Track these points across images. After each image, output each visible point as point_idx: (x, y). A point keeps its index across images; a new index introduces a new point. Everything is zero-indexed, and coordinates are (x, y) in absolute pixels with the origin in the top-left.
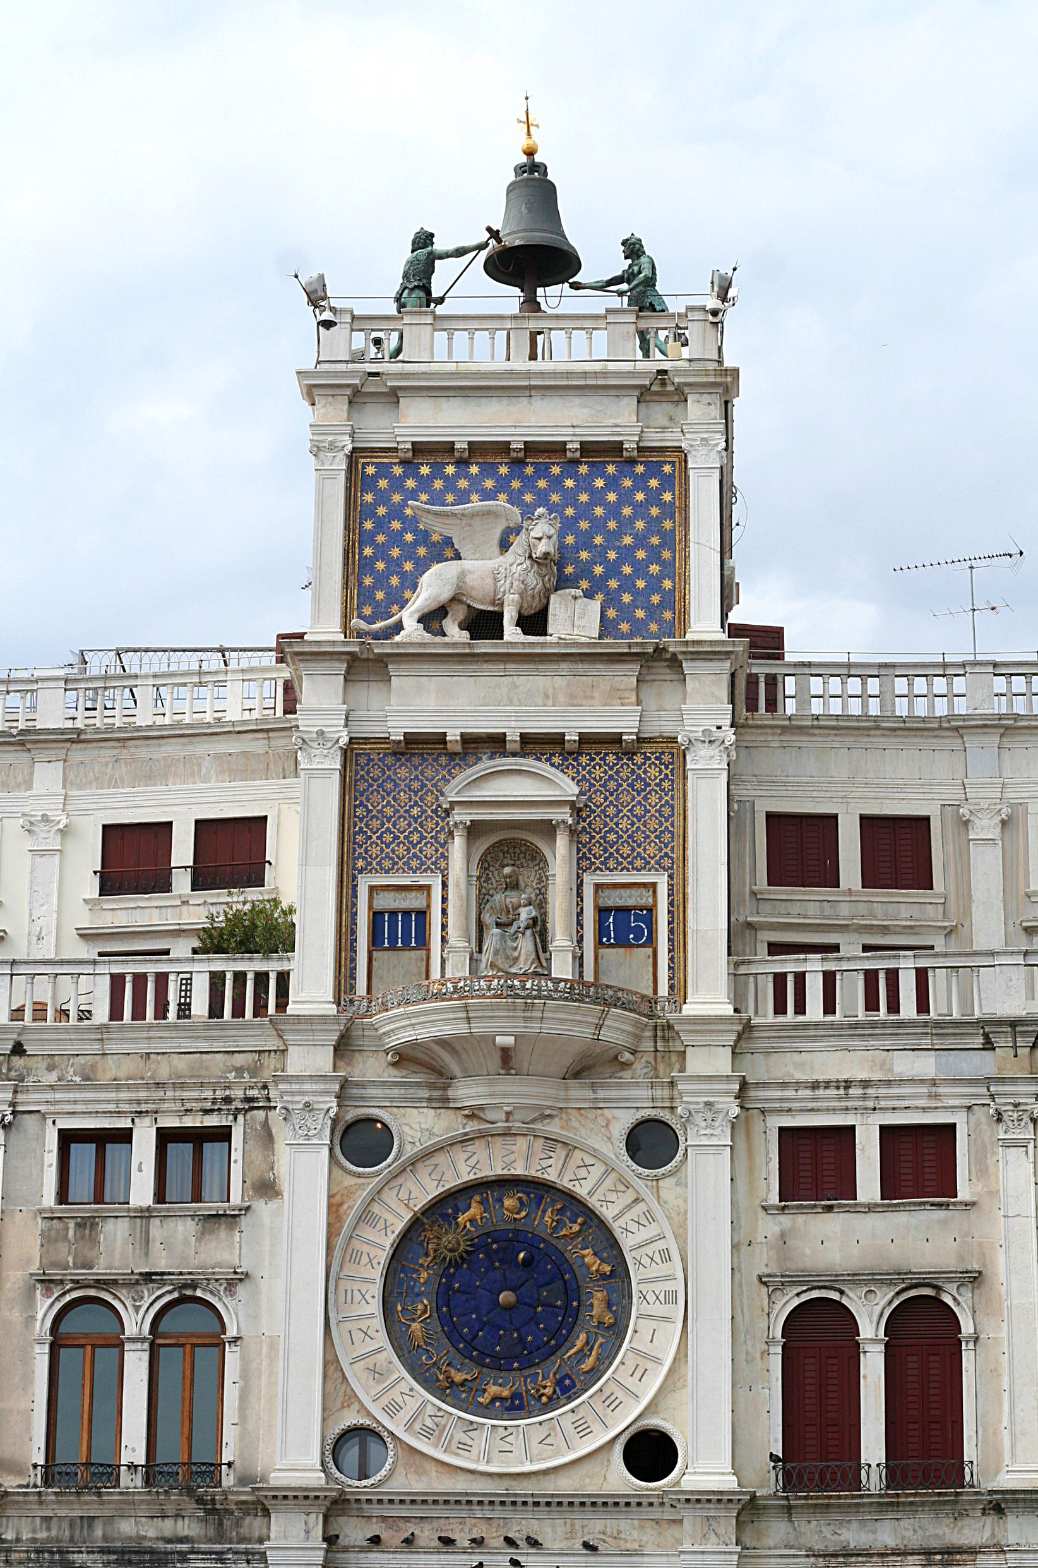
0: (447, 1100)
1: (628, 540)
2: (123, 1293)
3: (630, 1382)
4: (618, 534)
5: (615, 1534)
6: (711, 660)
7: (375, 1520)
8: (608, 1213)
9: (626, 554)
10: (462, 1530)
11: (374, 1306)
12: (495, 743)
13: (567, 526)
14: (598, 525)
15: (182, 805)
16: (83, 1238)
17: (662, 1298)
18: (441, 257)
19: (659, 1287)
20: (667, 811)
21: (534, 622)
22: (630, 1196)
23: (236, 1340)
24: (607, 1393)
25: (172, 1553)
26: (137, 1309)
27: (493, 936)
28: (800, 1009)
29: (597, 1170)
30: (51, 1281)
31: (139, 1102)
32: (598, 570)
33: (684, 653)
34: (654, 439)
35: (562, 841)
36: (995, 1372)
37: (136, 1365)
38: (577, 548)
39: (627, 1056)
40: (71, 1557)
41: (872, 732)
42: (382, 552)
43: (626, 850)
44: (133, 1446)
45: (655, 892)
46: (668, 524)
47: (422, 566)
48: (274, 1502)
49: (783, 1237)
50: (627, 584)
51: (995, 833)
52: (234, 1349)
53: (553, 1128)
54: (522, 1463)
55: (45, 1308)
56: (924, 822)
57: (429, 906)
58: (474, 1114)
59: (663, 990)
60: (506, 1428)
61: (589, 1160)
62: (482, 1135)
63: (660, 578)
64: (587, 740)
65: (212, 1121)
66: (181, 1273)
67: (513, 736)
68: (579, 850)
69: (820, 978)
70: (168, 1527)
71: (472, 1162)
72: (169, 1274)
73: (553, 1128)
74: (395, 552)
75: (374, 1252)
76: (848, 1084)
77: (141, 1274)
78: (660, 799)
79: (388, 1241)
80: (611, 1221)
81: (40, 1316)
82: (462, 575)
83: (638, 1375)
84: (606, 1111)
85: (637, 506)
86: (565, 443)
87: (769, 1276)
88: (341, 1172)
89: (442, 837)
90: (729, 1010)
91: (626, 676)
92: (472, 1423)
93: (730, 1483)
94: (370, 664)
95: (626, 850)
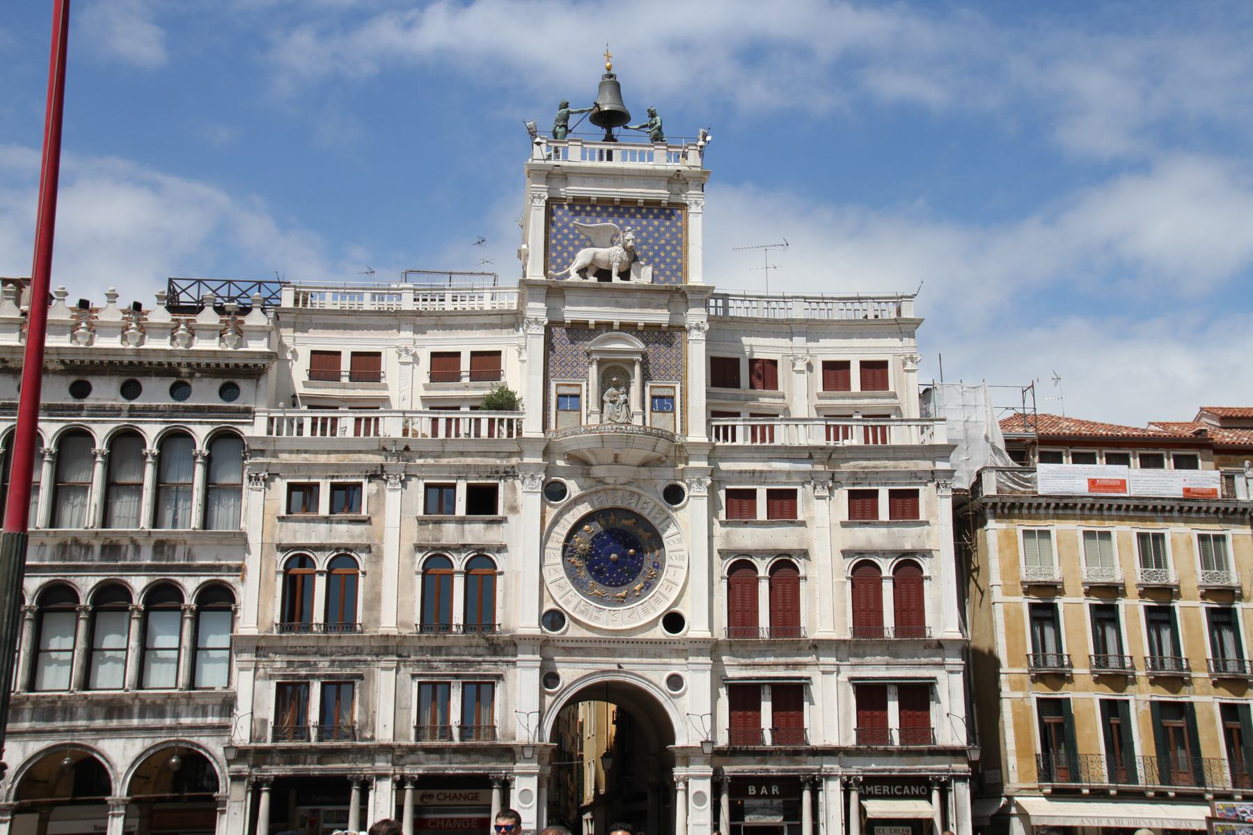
1: (663, 242)
3: (665, 593)
4: (658, 239)
8: (655, 523)
9: (662, 248)
11: (559, 560)
12: (609, 326)
13: (637, 234)
14: (650, 235)
15: (465, 343)
21: (625, 275)
22: (664, 516)
23: (501, 573)
27: (608, 406)
28: (734, 440)
29: (651, 506)
32: (651, 254)
34: (675, 200)
35: (637, 369)
37: (459, 584)
38: (642, 244)
42: (559, 242)
44: (458, 616)
47: (577, 249)
49: (727, 534)
50: (663, 260)
51: (804, 368)
55: (420, 558)
56: (774, 363)
58: (600, 481)
59: (678, 431)
63: (676, 258)
64: (647, 325)
67: (616, 324)
74: (565, 243)
76: (754, 472)
79: (565, 533)
82: (595, 254)
85: (667, 227)
90: (706, 440)
93: (708, 635)
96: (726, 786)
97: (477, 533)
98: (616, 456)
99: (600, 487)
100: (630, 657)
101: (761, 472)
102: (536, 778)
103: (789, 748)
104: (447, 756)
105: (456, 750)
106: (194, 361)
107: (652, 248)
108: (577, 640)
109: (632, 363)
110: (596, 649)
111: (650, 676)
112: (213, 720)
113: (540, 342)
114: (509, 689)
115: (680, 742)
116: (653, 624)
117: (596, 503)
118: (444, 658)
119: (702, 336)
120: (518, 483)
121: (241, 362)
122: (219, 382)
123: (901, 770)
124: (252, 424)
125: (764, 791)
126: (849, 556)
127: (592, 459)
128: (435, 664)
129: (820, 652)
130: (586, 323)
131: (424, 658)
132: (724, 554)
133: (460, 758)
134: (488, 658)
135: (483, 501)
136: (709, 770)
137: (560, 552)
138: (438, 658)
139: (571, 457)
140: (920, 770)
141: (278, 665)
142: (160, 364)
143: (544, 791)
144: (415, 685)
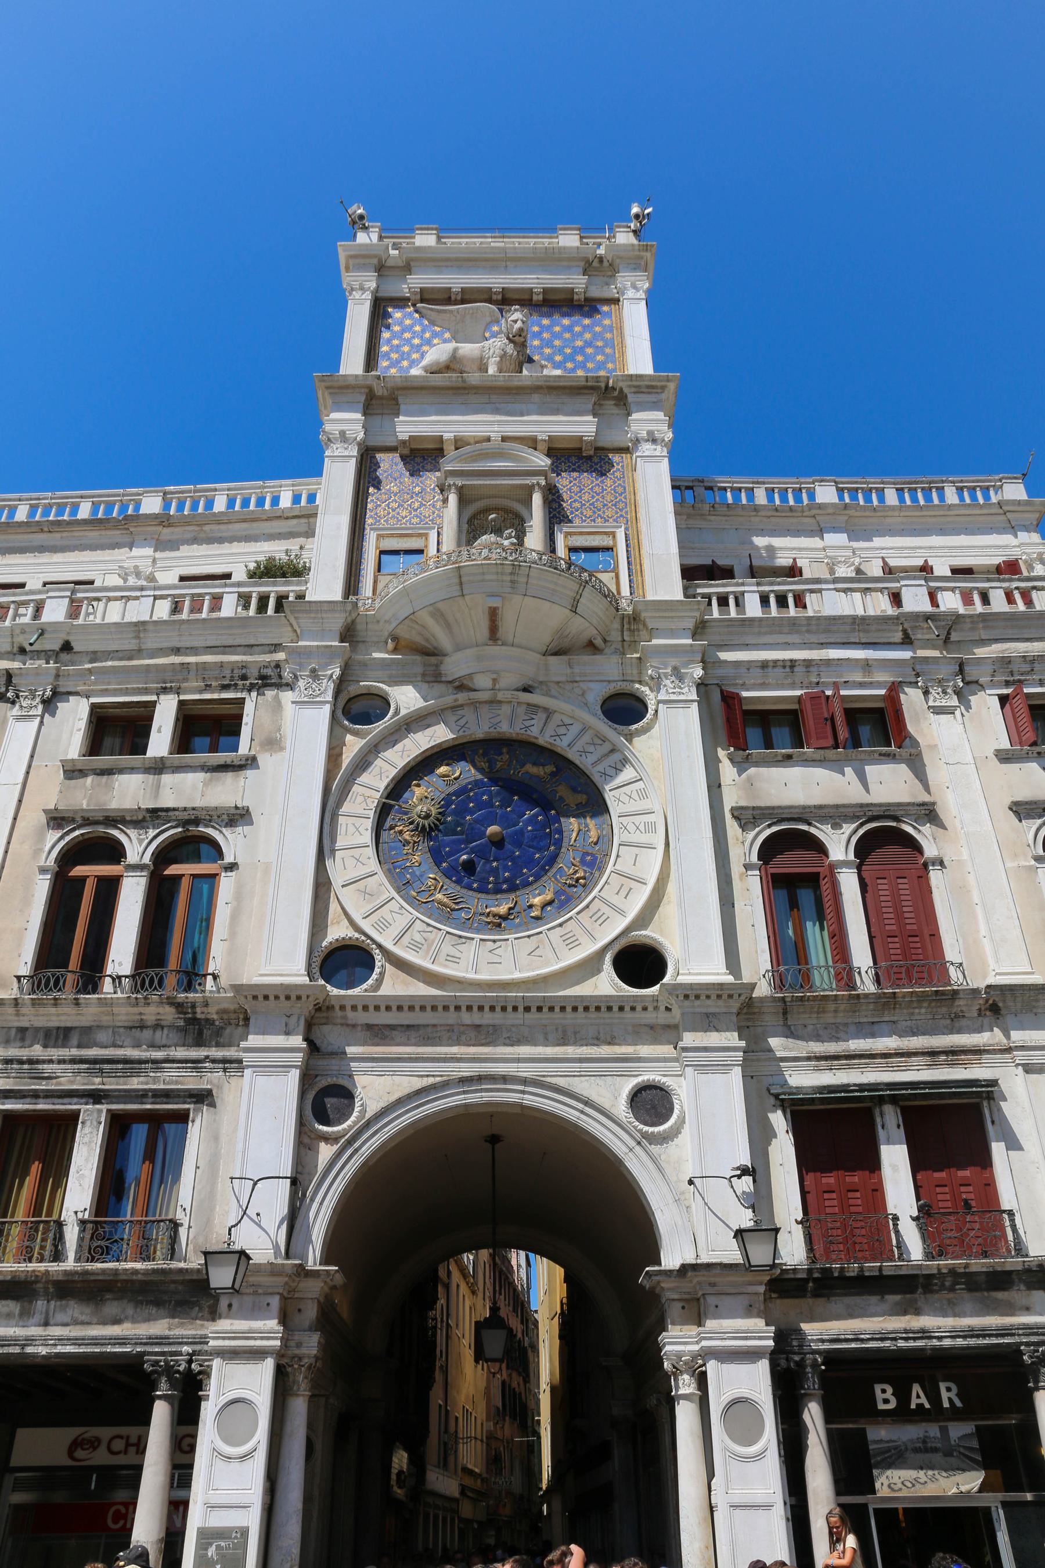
3: (615, 900)
5: (609, 1040)
6: (649, 393)
7: (359, 1028)
9: (581, 350)
10: (449, 1038)
11: (367, 837)
16: (98, 785)
17: (642, 827)
19: (637, 819)
20: (620, 490)
22: (607, 747)
23: (232, 867)
24: (594, 907)
25: (146, 1062)
26: (140, 841)
29: (574, 730)
30: (63, 819)
33: (630, 386)
34: (595, 292)
35: (537, 499)
36: (961, 890)
39: (598, 642)
40: (40, 1066)
41: (753, 519)
45: (614, 537)
46: (608, 336)
48: (254, 1002)
52: (229, 874)
54: (511, 973)
55: (54, 842)
57: (426, 546)
58: (461, 686)
59: (625, 591)
60: (494, 941)
61: (567, 721)
66: (185, 809)
68: (550, 513)
69: (756, 598)
71: (462, 722)
72: (174, 809)
75: (369, 792)
76: (793, 664)
77: (148, 810)
78: (615, 482)
80: (590, 767)
81: (47, 849)
83: (623, 893)
84: (581, 684)
85: (584, 327)
86: (531, 289)
87: (742, 808)
88: (342, 730)
89: (439, 504)
92: (460, 937)
94: (384, 402)
95: (590, 513)
96: (812, 1383)
97: (188, 789)
98: (493, 614)
99: (462, 697)
100: (534, 1043)
101: (808, 664)
102: (269, 1364)
103: (978, 1264)
104: (40, 1304)
105: (67, 1289)
107: (560, 351)
108: (400, 1005)
110: (450, 1028)
111: (591, 1091)
113: (351, 466)
114: (225, 1130)
115: (673, 1255)
116: (590, 967)
118: (75, 1052)
119: (660, 451)
120: (287, 697)
125: (918, 1397)
126: (1029, 816)
127: (444, 641)
129: (1010, 1019)
131: (24, 1053)
132: (747, 817)
133: (75, 1309)
134: (181, 1053)
135: (209, 729)
136: (759, 1332)
137: (369, 824)
138: (55, 1053)
139: (399, 645)
143: (299, 1407)
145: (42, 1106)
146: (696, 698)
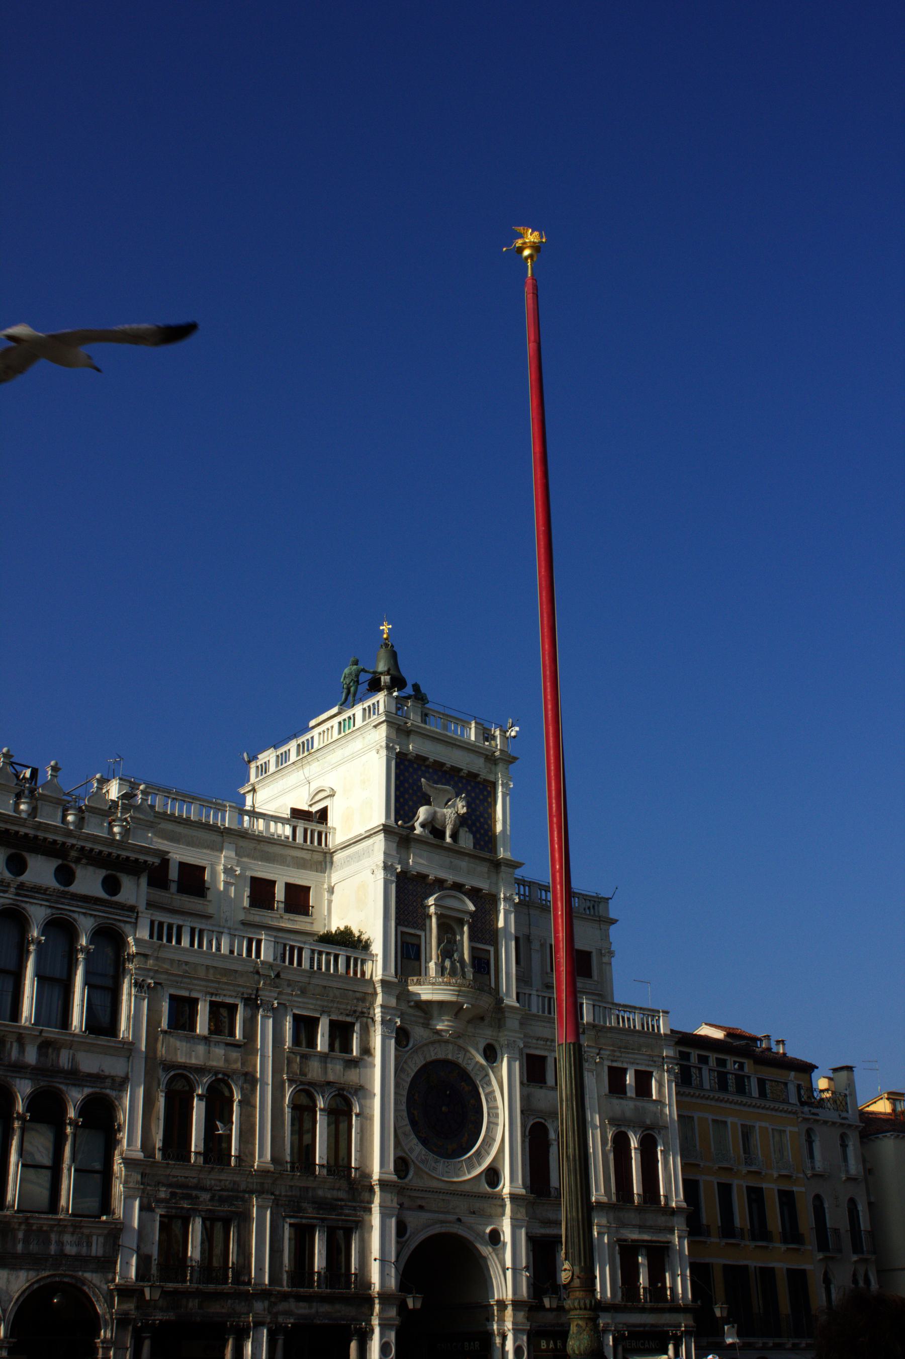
0: (428, 1024)
2: (318, 1089)
18: (366, 672)
19: (493, 1111)
22: (484, 1073)
26: (323, 1097)
31: (323, 1006)
43: (480, 935)
53: (460, 1042)
58: (438, 1032)
62: (439, 1041)
65: (349, 1019)
70: (335, 1194)
73: (460, 1042)
82: (435, 813)
91: (483, 868)
104: (315, 1304)
106: (88, 845)
109: (461, 922)
112: (97, 1249)
117: (433, 1054)
121: (133, 856)
122: (102, 873)
123: (652, 1325)
124: (136, 923)
128: (304, 1205)
130: (425, 877)
140: (663, 1325)
141: (162, 1195)
142: (55, 841)
144: (287, 1226)
145: (304, 1221)
146: (517, 1056)
